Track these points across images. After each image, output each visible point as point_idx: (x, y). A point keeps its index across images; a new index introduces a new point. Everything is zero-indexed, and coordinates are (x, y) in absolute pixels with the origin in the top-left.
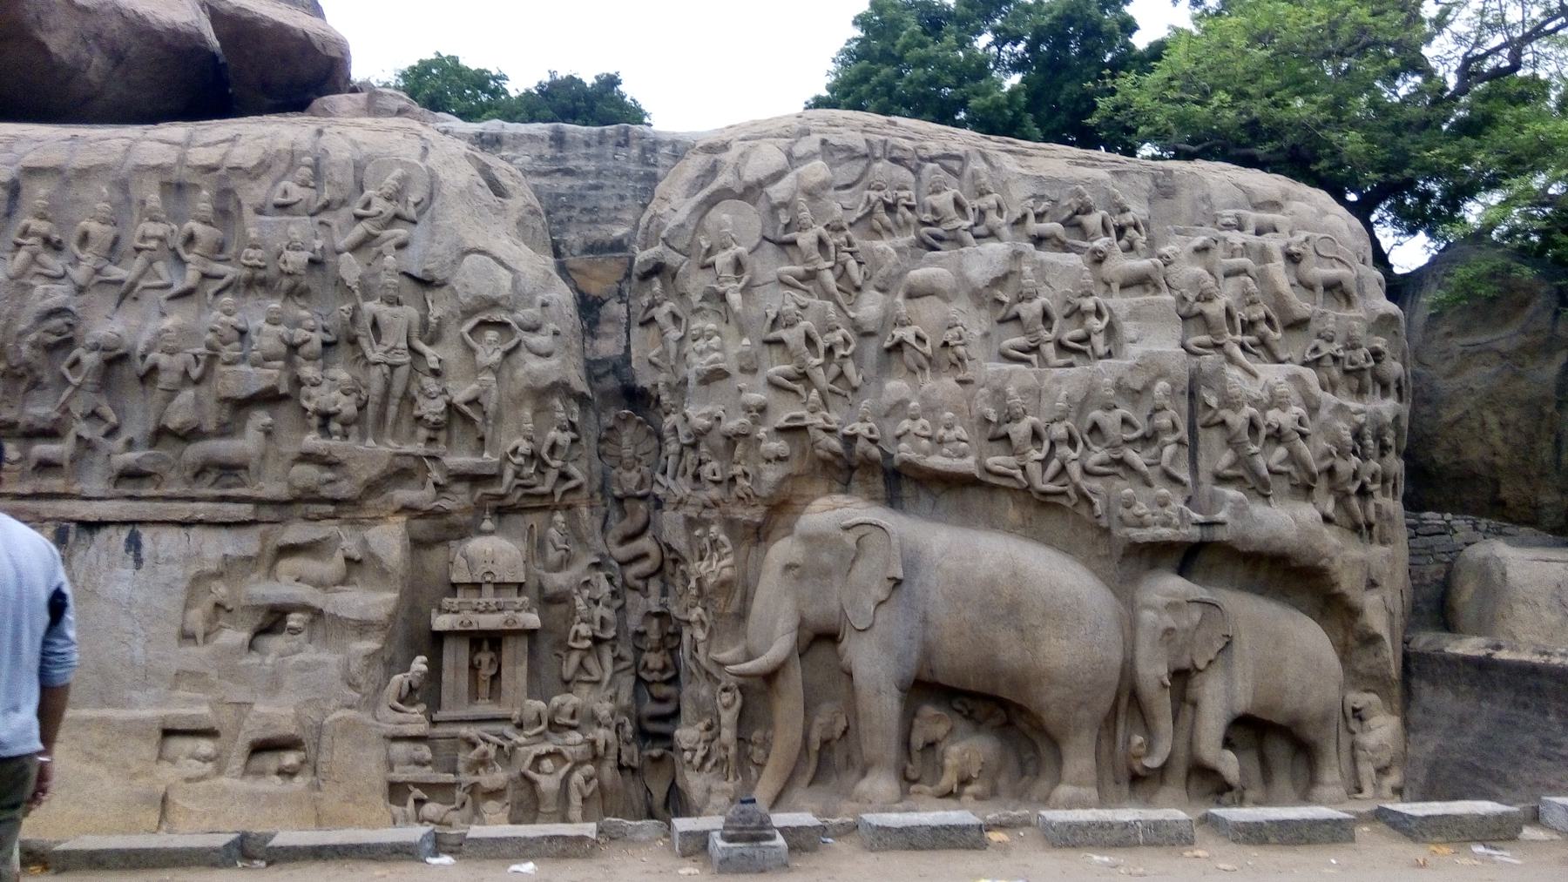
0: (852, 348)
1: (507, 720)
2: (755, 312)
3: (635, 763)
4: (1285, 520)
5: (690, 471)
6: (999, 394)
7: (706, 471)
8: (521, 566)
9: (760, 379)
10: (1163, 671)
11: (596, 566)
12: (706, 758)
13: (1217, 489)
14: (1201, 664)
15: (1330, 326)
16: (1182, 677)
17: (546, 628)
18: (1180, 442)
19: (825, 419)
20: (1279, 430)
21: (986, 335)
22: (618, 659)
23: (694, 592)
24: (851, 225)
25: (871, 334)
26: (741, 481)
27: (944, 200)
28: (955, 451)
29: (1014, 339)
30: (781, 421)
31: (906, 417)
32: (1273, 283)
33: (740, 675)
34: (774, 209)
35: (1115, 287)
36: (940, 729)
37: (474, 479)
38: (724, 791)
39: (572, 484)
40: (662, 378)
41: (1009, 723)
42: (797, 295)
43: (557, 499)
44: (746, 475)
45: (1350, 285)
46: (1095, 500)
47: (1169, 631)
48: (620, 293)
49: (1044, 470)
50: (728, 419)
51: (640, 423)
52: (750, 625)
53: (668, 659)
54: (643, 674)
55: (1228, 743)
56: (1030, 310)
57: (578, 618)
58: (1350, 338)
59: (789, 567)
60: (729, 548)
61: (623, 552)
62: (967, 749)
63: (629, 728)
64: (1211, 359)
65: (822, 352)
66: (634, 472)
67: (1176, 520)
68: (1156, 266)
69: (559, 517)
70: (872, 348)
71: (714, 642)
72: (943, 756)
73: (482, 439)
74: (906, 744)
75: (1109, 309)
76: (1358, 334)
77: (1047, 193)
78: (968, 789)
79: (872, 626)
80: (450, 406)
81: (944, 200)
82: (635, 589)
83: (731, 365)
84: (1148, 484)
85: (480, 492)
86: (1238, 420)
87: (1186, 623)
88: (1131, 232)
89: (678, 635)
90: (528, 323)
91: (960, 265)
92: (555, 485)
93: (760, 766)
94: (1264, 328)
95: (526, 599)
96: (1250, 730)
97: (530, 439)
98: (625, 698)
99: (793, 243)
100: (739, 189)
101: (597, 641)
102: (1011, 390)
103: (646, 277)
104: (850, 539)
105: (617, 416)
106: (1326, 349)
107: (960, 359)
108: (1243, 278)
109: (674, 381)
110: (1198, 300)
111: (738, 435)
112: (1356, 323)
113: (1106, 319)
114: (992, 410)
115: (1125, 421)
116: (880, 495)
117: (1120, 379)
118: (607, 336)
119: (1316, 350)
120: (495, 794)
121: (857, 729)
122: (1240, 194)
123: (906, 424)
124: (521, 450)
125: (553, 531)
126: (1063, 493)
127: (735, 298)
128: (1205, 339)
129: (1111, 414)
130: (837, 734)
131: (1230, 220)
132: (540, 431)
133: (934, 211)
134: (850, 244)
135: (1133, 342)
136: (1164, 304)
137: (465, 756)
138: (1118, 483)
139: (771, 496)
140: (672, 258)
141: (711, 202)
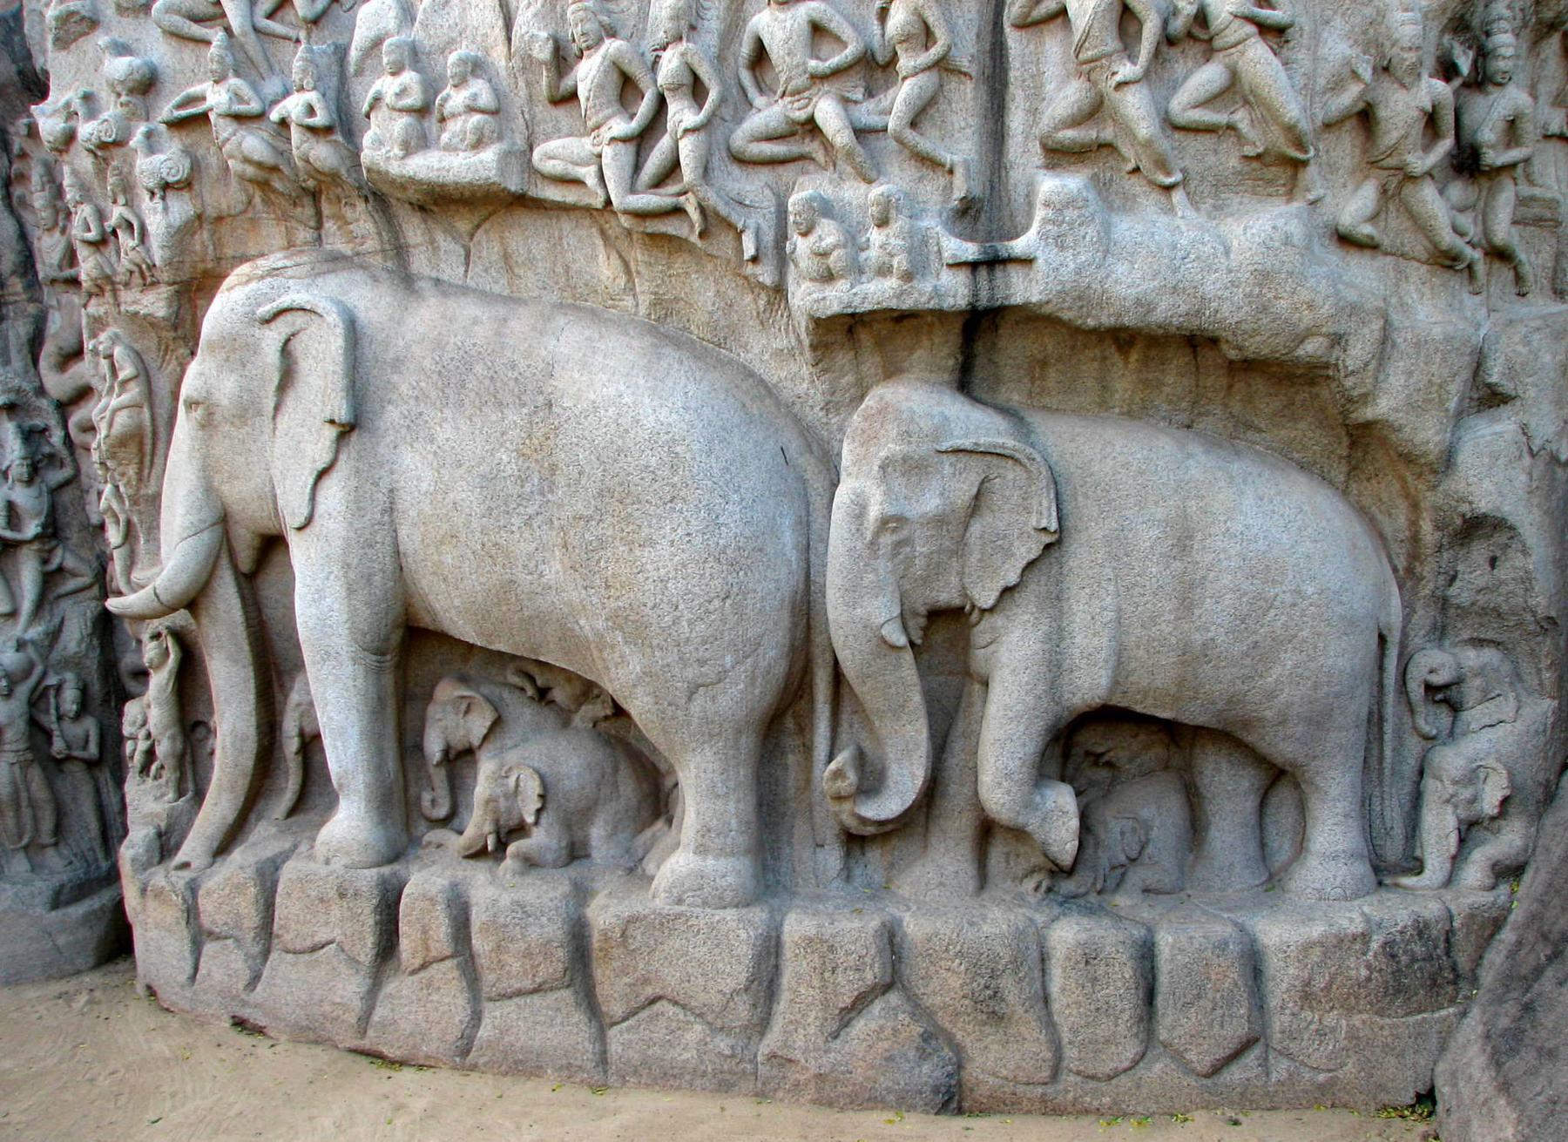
10: (881, 611)
12: (150, 754)
14: (986, 598)
18: (943, 66)
19: (237, 97)
20: (1202, 18)
30: (167, 109)
49: (637, 168)
50: (92, 114)
59: (192, 404)
61: (57, 384)
62: (520, 767)
74: (408, 746)
78: (511, 848)
104: (271, 339)
111: (103, 146)
116: (371, 244)
126: (678, 211)
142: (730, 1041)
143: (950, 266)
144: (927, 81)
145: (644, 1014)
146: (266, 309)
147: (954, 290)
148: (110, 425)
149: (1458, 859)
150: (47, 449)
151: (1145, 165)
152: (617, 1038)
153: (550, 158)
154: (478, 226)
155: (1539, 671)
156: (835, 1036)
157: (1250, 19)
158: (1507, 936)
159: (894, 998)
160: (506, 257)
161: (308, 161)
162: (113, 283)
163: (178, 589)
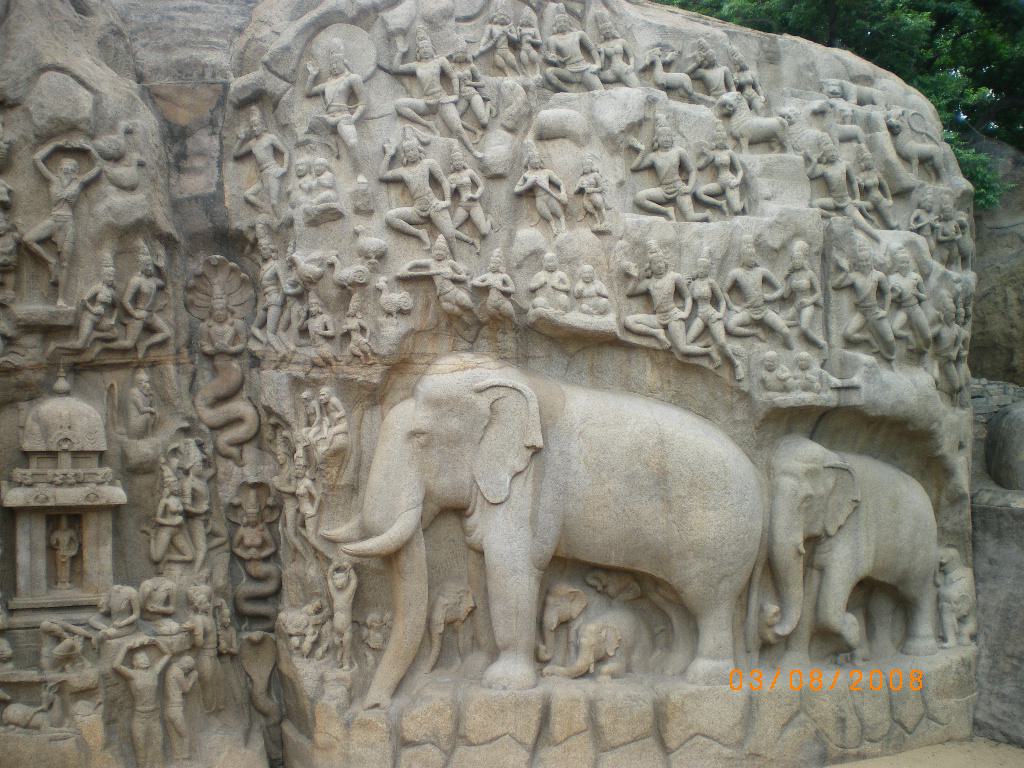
0: (480, 190)
1: (92, 607)
2: (371, 148)
3: (234, 649)
4: (908, 386)
5: (296, 324)
6: (639, 247)
7: (315, 325)
8: (101, 431)
9: (376, 223)
10: (798, 538)
11: (186, 431)
12: (316, 644)
13: (849, 353)
14: (832, 530)
15: (929, 196)
16: (813, 542)
17: (132, 504)
19: (453, 268)
20: (900, 296)
21: (621, 184)
22: (211, 535)
23: (302, 462)
24: (474, 58)
25: (499, 177)
26: (356, 336)
27: (570, 40)
28: (596, 307)
29: (650, 191)
30: (404, 269)
31: (540, 267)
32: (883, 152)
33: (359, 556)
34: (390, 37)
35: (744, 142)
36: (575, 608)
37: (47, 330)
38: (339, 680)
39: (158, 338)
40: (261, 219)
41: (643, 596)
42: (418, 130)
43: (140, 356)
44: (362, 330)
45: (938, 160)
46: (738, 362)
47: (808, 498)
48: (212, 123)
50: (344, 265)
51: (233, 270)
52: (368, 499)
53: (267, 534)
54: (239, 551)
55: (850, 607)
56: (666, 160)
57: (167, 491)
58: (942, 211)
59: (414, 434)
60: (342, 412)
62: (604, 625)
63: (227, 611)
64: (837, 220)
65: (448, 194)
66: (226, 327)
67: (817, 385)
68: (782, 124)
69: (143, 376)
70: (501, 193)
71: (325, 516)
72: (577, 636)
73: (55, 284)
75: (743, 165)
76: (950, 206)
77: (671, 43)
78: (606, 668)
79: (507, 499)
80: (21, 247)
81: (570, 40)
82: (228, 457)
83: (344, 205)
84: (786, 345)
85: (52, 346)
86: (866, 283)
87: (822, 490)
88: (749, 91)
89: (278, 507)
90: (111, 151)
91: (591, 108)
92: (139, 340)
93: (378, 651)
94: (877, 194)
95: (108, 470)
96: (869, 592)
97: (111, 286)
98: (221, 580)
99: (412, 74)
100: (352, 13)
101: (189, 516)
102: (653, 242)
103: (243, 105)
104: (483, 402)
105: (208, 262)
106: (927, 219)
107: (597, 208)
108: (855, 144)
109: (276, 222)
110: (819, 161)
111: (354, 284)
112: (947, 196)
113: (740, 174)
114: (633, 265)
115: (766, 281)
117: (759, 236)
118: (197, 171)
119: (917, 220)
120: (85, 693)
121: (487, 608)
122: (840, 67)
123: (542, 276)
124: (102, 297)
125: (136, 391)
126: (707, 355)
127: (348, 131)
128: (829, 201)
129: (752, 273)
130: (463, 615)
131: (837, 89)
132: (121, 276)
133: (559, 51)
134: (474, 78)
135: (768, 199)
136: (794, 162)
137: (50, 651)
138: (760, 344)
139: (391, 354)
140: (274, 85)
141: (320, 25)
142: (728, 751)
143: (832, 388)
144: (812, 307)
145: (688, 744)
146: (481, 384)
147: (829, 398)
148: (331, 443)
149: (958, 634)
150: (205, 457)
151: (883, 351)
152: (676, 759)
153: (638, 323)
154: (579, 351)
155: (966, 556)
156: (778, 739)
157: (918, 298)
158: (983, 661)
159: (802, 716)
160: (592, 368)
161: (498, 309)
162: (337, 361)
163: (405, 539)
